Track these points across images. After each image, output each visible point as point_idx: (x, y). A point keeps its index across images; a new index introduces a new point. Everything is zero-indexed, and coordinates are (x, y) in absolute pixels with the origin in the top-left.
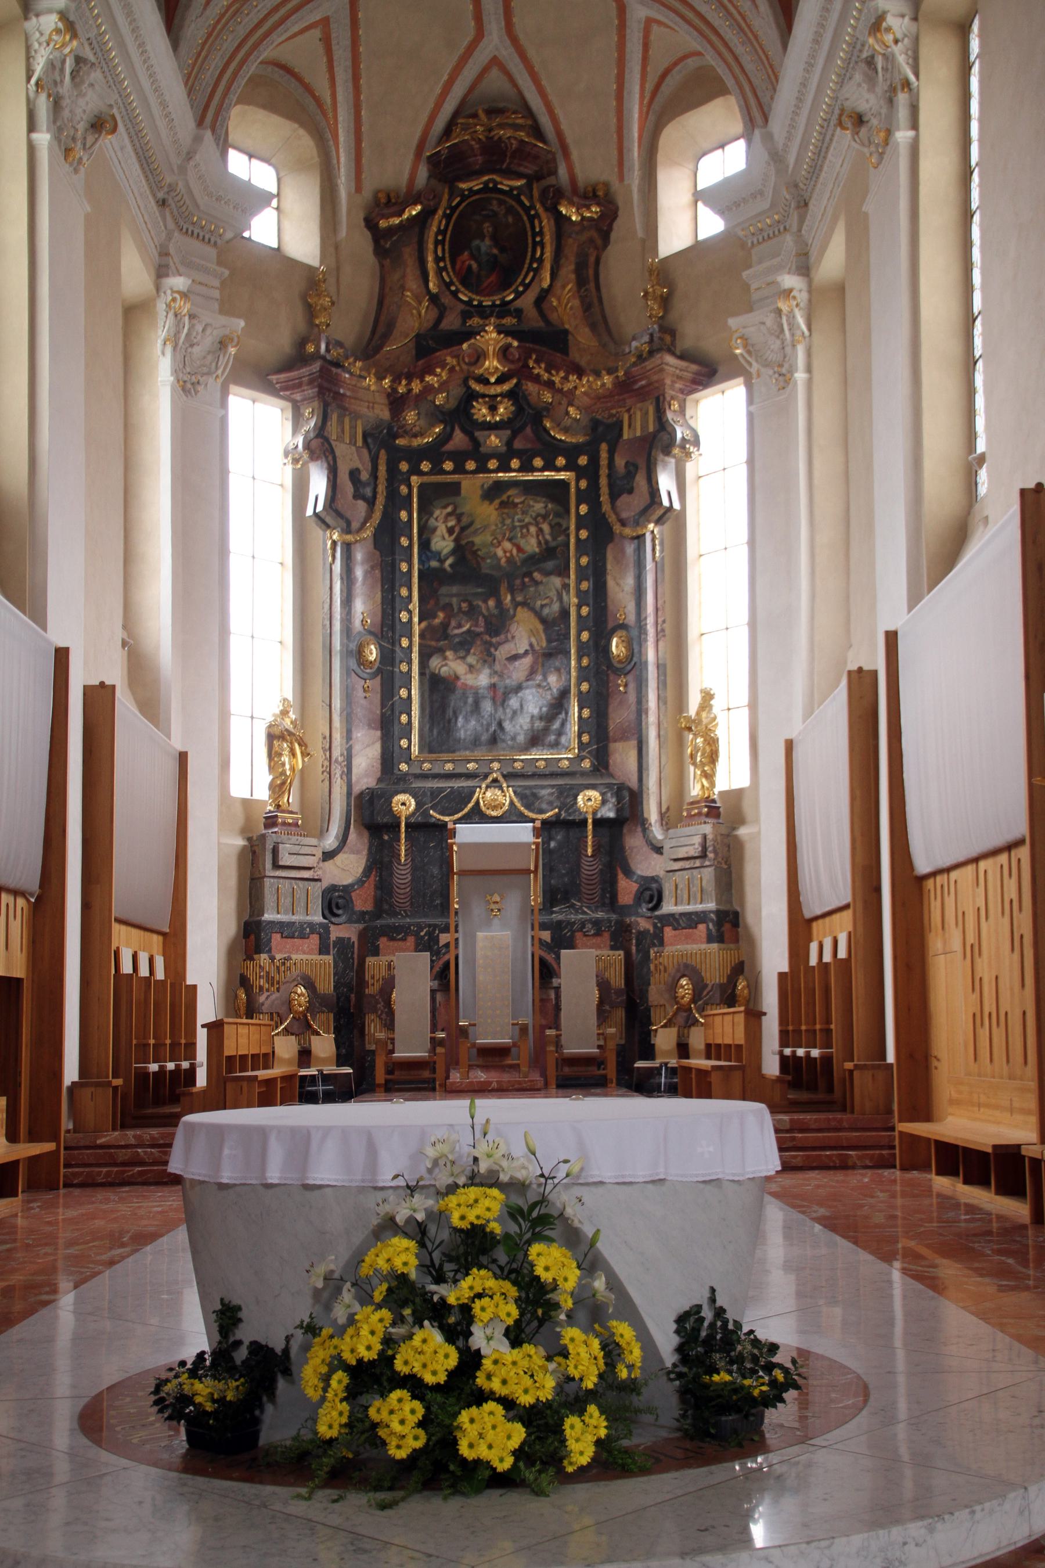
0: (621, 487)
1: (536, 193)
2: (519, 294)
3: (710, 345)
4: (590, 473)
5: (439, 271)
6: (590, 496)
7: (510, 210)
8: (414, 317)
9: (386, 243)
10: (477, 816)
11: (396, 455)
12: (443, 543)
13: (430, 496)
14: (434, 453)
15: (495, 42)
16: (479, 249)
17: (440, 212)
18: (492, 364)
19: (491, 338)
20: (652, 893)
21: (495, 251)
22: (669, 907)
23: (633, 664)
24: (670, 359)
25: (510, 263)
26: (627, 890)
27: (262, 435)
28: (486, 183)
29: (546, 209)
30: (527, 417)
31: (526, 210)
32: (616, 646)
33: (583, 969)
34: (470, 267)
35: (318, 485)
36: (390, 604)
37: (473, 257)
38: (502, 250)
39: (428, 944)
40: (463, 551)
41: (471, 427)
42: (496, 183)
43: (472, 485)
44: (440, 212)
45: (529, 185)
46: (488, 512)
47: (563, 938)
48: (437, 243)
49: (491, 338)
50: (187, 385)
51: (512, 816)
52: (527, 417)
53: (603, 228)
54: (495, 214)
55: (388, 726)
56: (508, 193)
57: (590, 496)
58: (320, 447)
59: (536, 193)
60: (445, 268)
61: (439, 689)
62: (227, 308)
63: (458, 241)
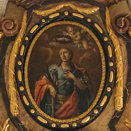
1: (108, 21)
2: (94, 117)
5: (20, 94)
7: (84, 36)
16: (56, 73)
17: (19, 39)
21: (71, 76)
28: (61, 12)
29: (118, 35)
31: (100, 37)
34: (48, 91)
37: (50, 81)
38: (78, 74)
42: (71, 11)
44: (19, 39)
45: (102, 13)
48: (17, 68)
54: (71, 41)
56: (83, 21)
59: (108, 21)
60: (25, 93)
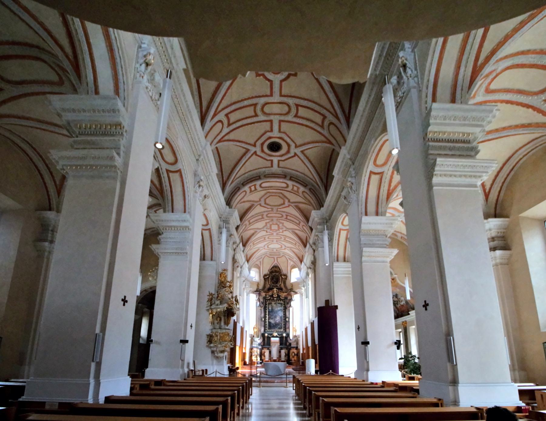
0: (288, 303)
3: (296, 291)
4: (285, 302)
6: (284, 304)
8: (268, 286)
9: (265, 279)
10: (273, 337)
11: (266, 300)
12: (270, 308)
13: (269, 304)
14: (269, 300)
15: (276, 262)
18: (275, 292)
19: (275, 289)
20: (290, 344)
22: (292, 346)
23: (289, 321)
24: (292, 293)
25: (277, 281)
26: (288, 344)
27: (253, 298)
30: (279, 296)
32: (287, 319)
33: (283, 352)
35: (258, 303)
36: (265, 314)
39: (268, 349)
40: (272, 309)
41: (273, 297)
43: (273, 303)
46: (274, 305)
47: (281, 349)
49: (275, 289)
50: (247, 295)
51: (277, 337)
52: (279, 296)
53: (286, 279)
55: (265, 327)
57: (284, 304)
58: (259, 300)
61: (269, 323)
62: (251, 287)
63: (272, 279)
